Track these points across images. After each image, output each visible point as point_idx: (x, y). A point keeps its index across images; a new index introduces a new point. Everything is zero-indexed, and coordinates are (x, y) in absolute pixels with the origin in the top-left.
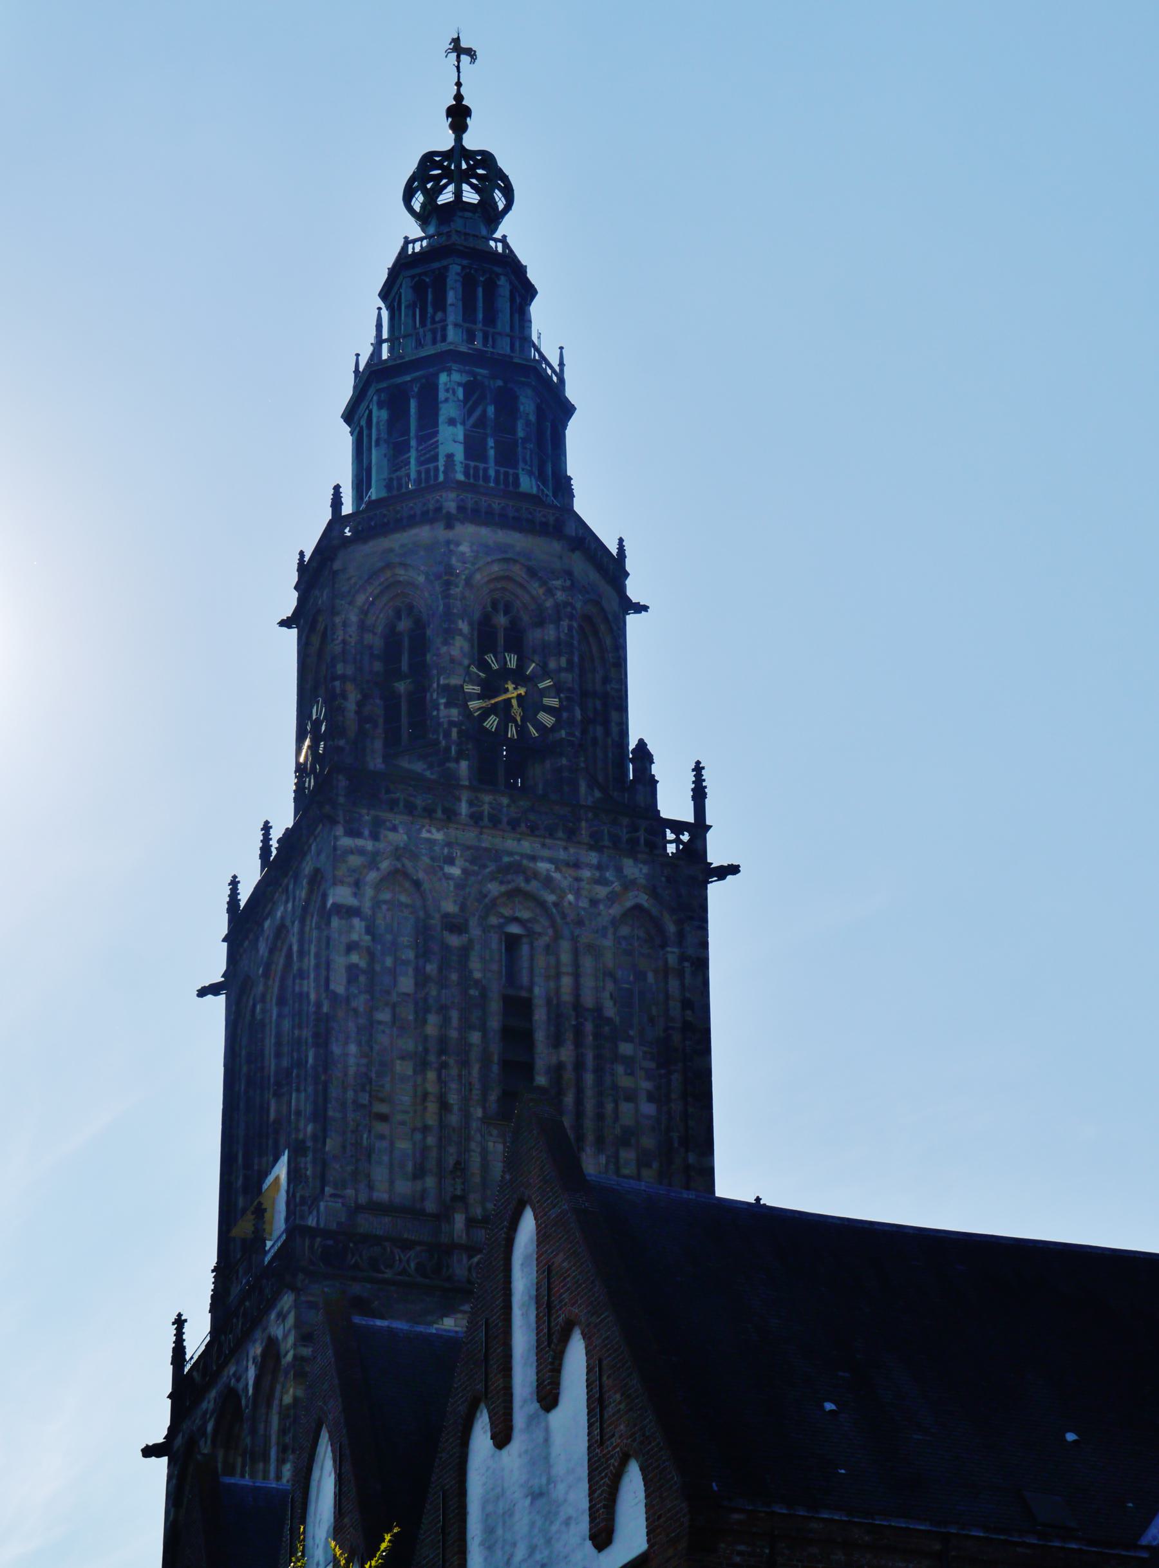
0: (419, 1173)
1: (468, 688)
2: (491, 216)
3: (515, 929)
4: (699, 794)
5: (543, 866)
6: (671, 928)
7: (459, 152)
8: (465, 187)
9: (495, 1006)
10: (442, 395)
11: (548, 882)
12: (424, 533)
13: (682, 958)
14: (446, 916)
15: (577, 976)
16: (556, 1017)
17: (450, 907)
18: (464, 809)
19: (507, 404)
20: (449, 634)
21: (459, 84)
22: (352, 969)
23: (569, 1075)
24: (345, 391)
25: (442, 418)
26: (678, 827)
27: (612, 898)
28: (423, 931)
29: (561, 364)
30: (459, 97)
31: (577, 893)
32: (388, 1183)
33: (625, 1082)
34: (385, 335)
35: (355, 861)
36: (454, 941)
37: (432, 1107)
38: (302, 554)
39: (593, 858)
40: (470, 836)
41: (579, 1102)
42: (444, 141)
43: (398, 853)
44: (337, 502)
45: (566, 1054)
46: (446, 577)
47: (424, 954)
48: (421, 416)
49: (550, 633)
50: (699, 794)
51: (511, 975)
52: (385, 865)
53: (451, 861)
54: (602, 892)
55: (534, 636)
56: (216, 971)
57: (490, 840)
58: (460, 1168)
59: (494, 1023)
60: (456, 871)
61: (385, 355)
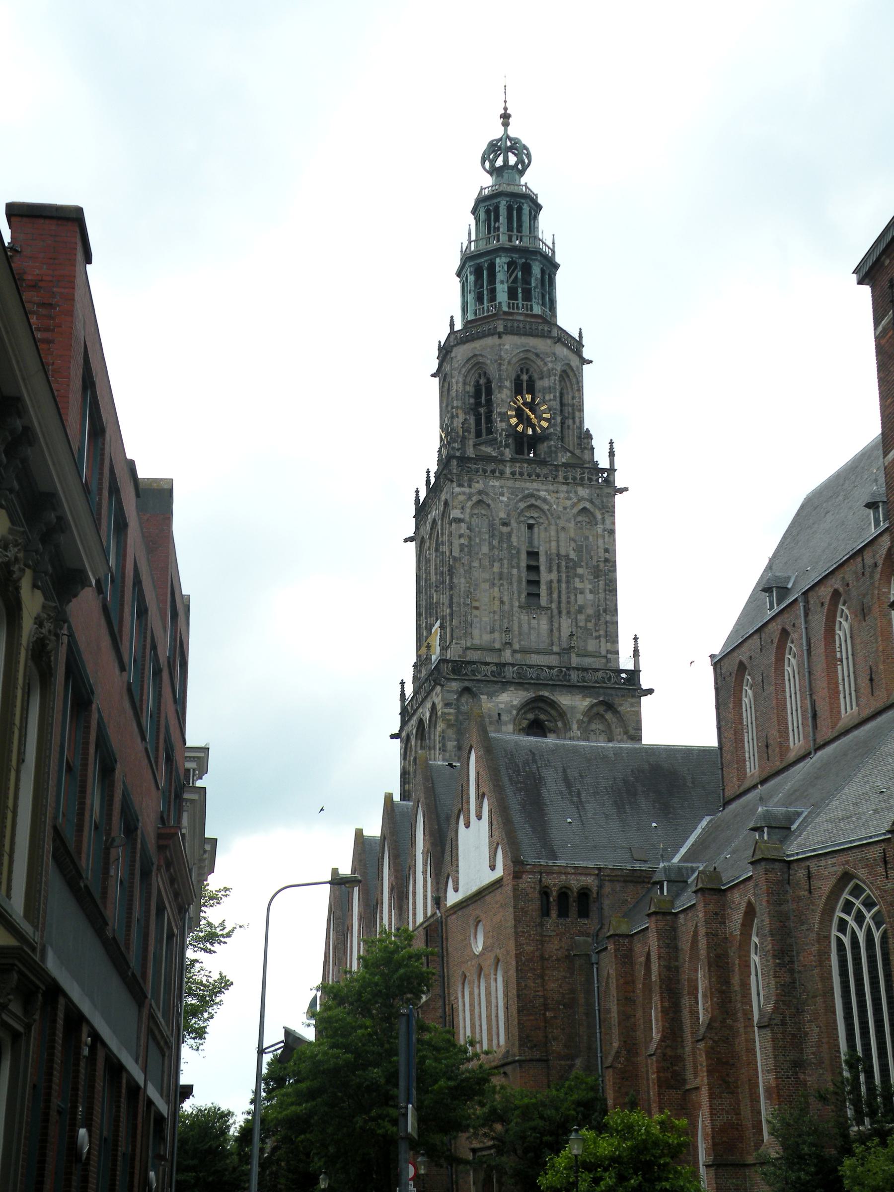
0: (492, 631)
1: (510, 413)
2: (521, 168)
3: (531, 521)
4: (612, 454)
5: (542, 494)
6: (599, 517)
8: (510, 154)
9: (524, 556)
10: (497, 269)
11: (545, 500)
12: (490, 341)
13: (604, 530)
14: (501, 519)
15: (558, 541)
16: (550, 560)
17: (502, 515)
18: (508, 470)
19: (527, 269)
20: (501, 388)
21: (505, 102)
22: (462, 546)
23: (555, 585)
24: (457, 263)
25: (497, 281)
26: (603, 470)
27: (574, 505)
28: (491, 526)
29: (553, 243)
30: (506, 109)
31: (558, 505)
32: (480, 637)
33: (579, 585)
34: (473, 237)
35: (461, 498)
36: (505, 530)
37: (497, 603)
38: (440, 342)
39: (564, 488)
40: (510, 483)
41: (559, 597)
43: (480, 492)
44: (452, 325)
45: (554, 576)
46: (499, 361)
47: (492, 536)
48: (489, 276)
49: (546, 383)
50: (612, 454)
51: (531, 542)
52: (475, 499)
53: (502, 494)
54: (568, 503)
55: (539, 384)
56: (410, 531)
57: (518, 484)
58: (508, 631)
59: (523, 564)
60: (505, 499)
61: (473, 249)
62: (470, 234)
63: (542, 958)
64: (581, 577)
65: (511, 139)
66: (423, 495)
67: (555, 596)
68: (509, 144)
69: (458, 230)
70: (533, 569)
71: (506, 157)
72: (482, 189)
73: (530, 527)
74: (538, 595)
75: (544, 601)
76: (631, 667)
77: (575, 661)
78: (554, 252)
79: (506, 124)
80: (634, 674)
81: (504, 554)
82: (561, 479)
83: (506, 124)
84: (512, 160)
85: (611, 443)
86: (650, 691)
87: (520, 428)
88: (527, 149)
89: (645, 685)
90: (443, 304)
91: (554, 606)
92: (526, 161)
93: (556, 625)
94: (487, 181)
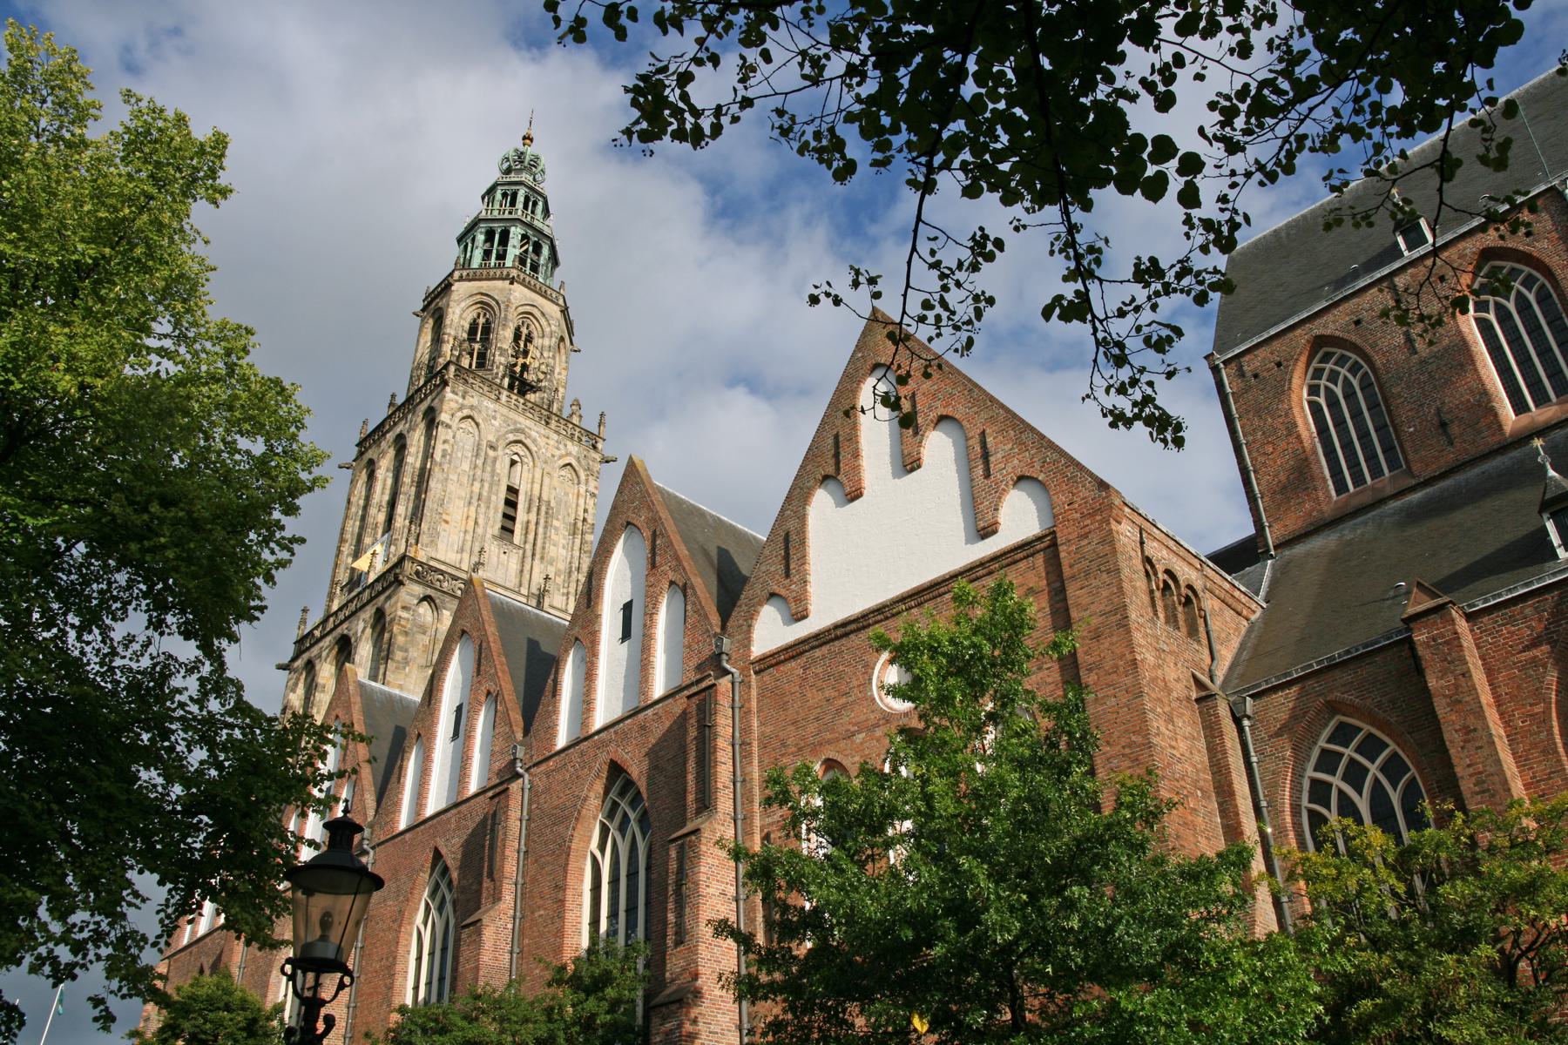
3: (516, 458)
5: (534, 434)
6: (583, 477)
9: (504, 488)
11: (534, 441)
17: (492, 438)
19: (537, 249)
23: (532, 527)
27: (561, 457)
35: (453, 405)
36: (491, 453)
37: (471, 523)
39: (555, 437)
40: (505, 411)
43: (472, 408)
45: (533, 517)
52: (466, 412)
57: (512, 415)
60: (496, 423)
64: (556, 529)
67: (531, 537)
70: (511, 504)
73: (513, 463)
74: (512, 532)
75: (518, 537)
81: (487, 476)
91: (529, 547)
93: (527, 567)
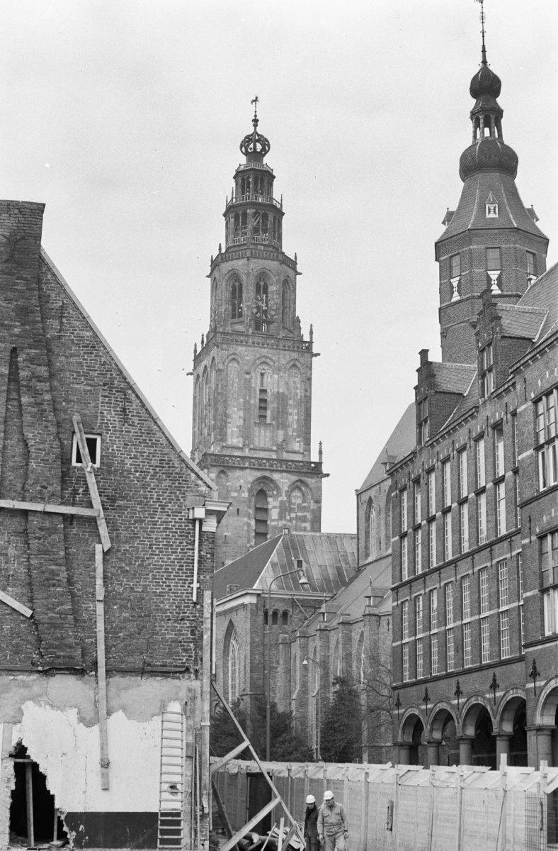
3: (263, 372)
4: (311, 333)
7: (256, 132)
18: (250, 341)
26: (306, 342)
29: (281, 200)
30: (256, 116)
34: (234, 196)
36: (248, 376)
38: (212, 256)
42: (251, 130)
44: (220, 249)
48: (243, 219)
50: (311, 333)
62: (233, 193)
63: (264, 645)
65: (258, 135)
66: (199, 349)
68: (257, 138)
69: (226, 189)
71: (255, 146)
72: (240, 165)
73: (262, 375)
74: (265, 417)
76: (317, 460)
77: (285, 456)
78: (281, 206)
79: (255, 126)
80: (319, 465)
82: (281, 347)
83: (255, 126)
84: (259, 147)
85: (311, 326)
86: (328, 475)
87: (258, 315)
88: (268, 141)
89: (324, 472)
90: (215, 236)
92: (267, 148)
94: (243, 160)
